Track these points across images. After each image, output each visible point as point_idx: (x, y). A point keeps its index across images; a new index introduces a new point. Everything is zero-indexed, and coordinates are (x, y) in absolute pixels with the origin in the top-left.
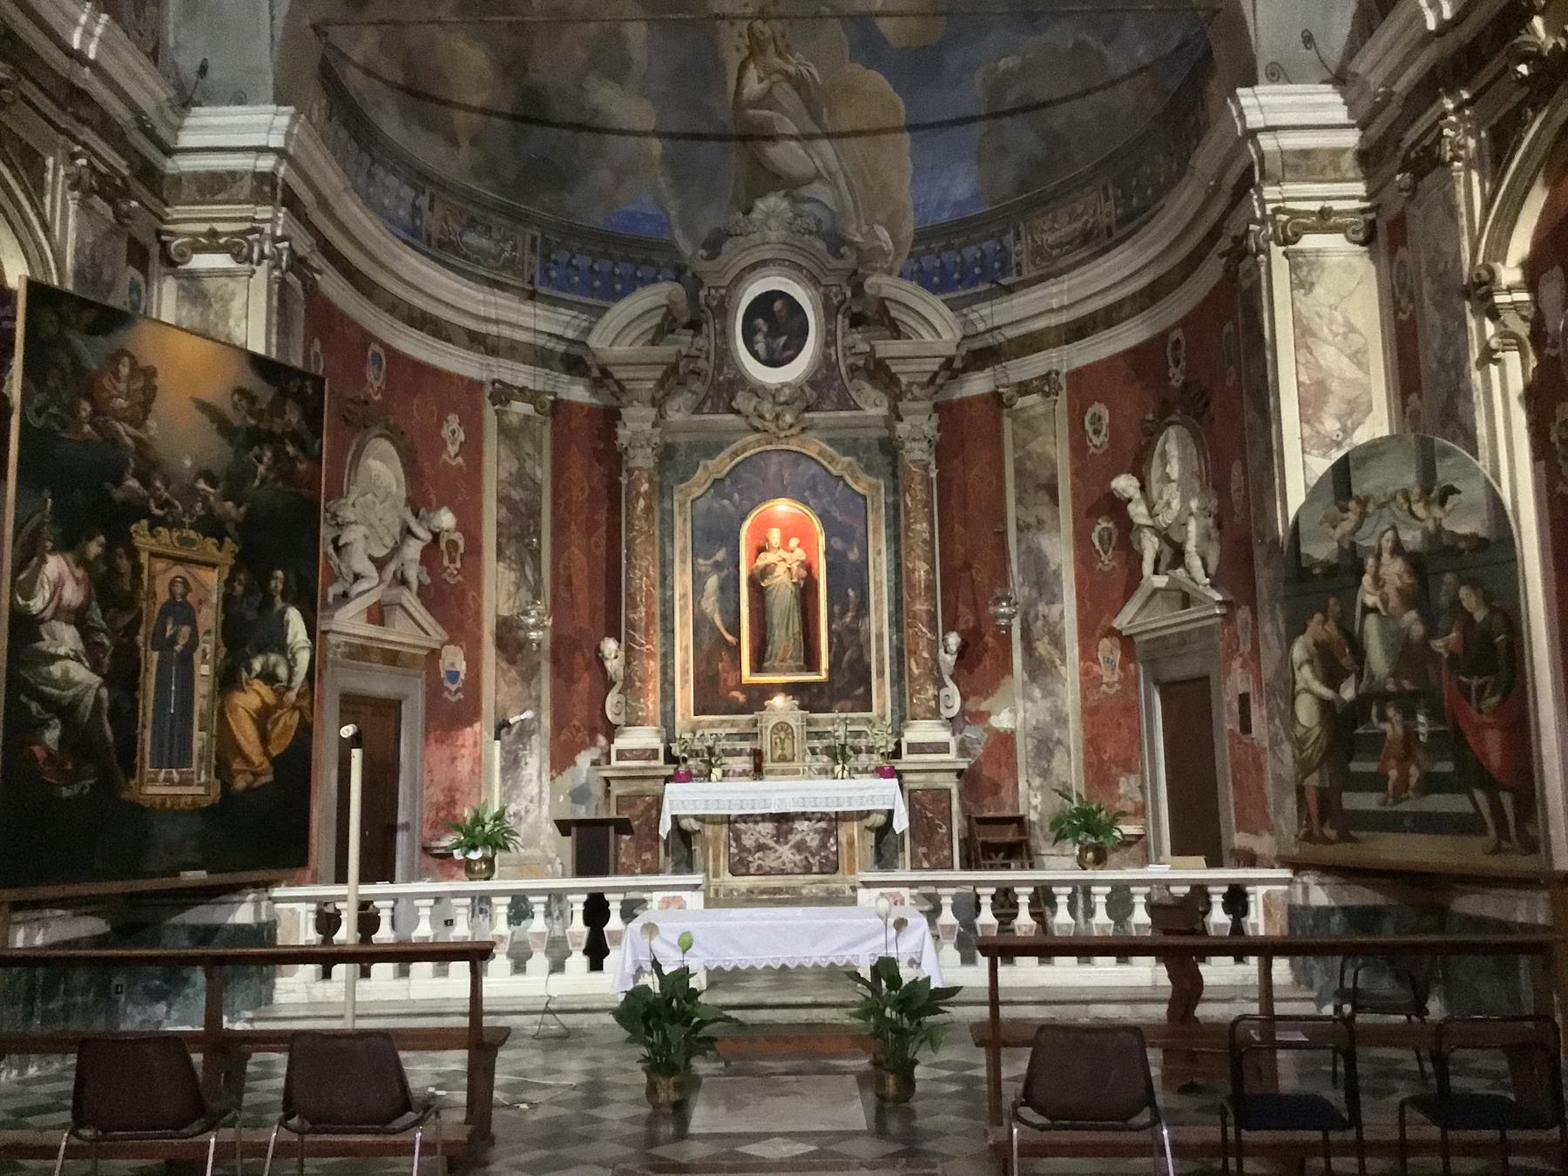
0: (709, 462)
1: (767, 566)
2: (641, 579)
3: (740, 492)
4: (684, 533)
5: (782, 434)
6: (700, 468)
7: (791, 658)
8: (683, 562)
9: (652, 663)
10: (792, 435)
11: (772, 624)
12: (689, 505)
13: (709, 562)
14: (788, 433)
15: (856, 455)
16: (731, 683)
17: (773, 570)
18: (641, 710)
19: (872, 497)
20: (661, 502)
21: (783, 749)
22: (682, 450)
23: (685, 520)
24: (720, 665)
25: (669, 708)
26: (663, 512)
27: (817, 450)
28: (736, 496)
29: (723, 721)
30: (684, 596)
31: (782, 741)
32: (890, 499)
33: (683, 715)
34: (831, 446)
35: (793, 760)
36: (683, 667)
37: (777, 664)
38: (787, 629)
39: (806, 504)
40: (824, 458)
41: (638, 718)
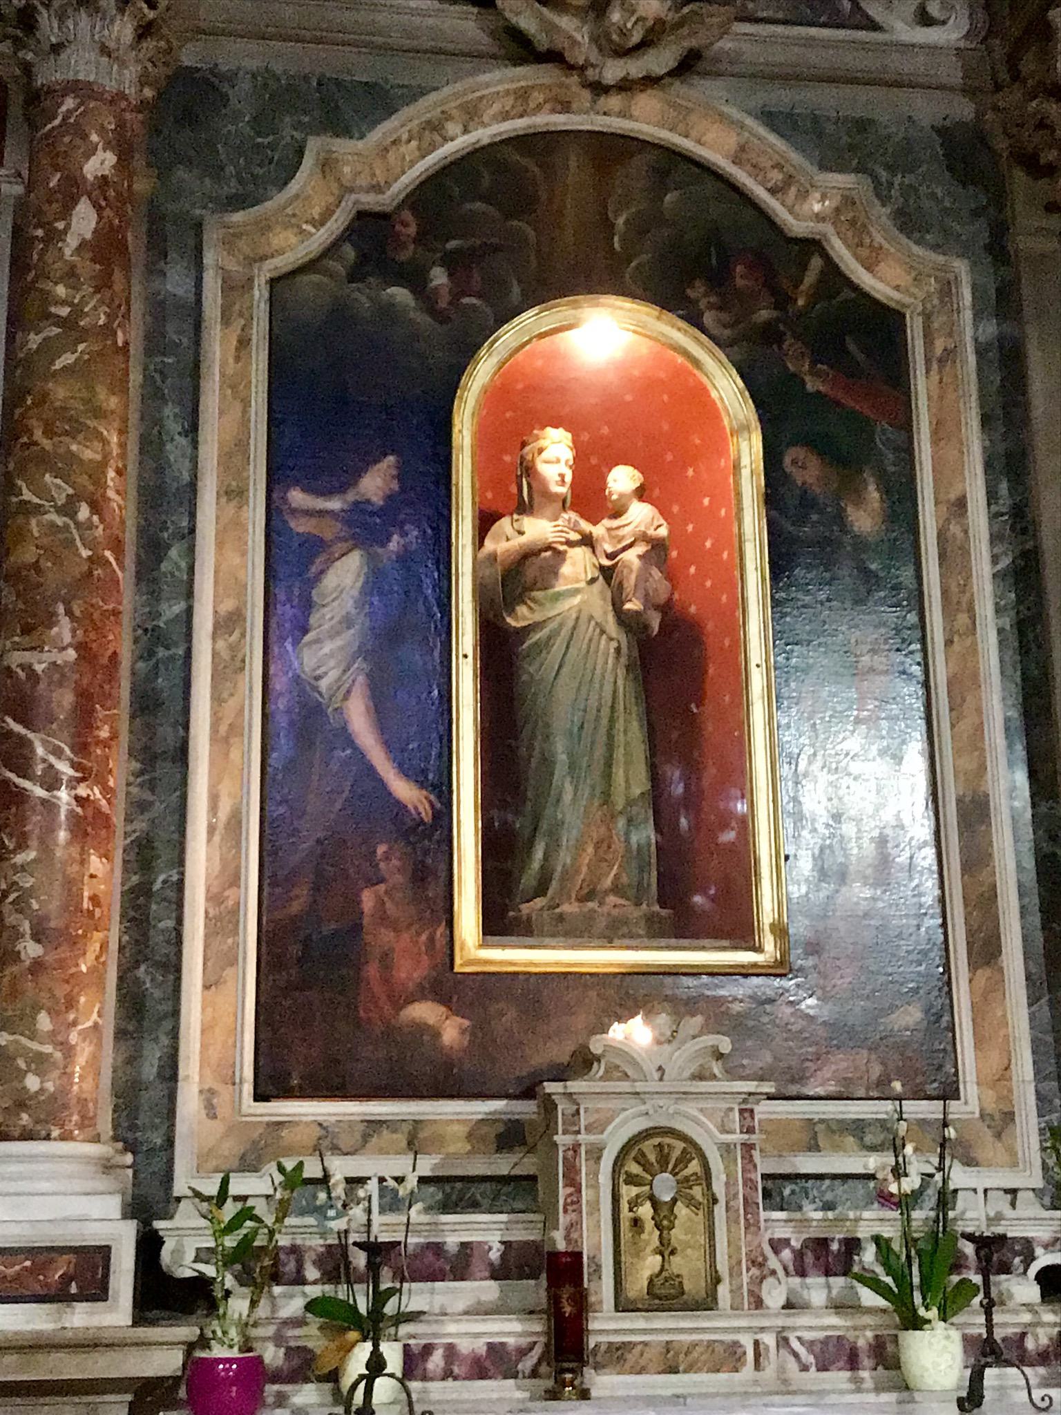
0: (343, 147)
1: (528, 555)
2: (68, 510)
3: (452, 262)
4: (236, 387)
5: (613, 71)
6: (308, 161)
7: (616, 889)
8: (234, 494)
9: (96, 864)
10: (650, 81)
11: (548, 762)
12: (260, 293)
13: (335, 504)
14: (634, 68)
15: (860, 169)
16: (410, 971)
17: (552, 571)
18: (40, 1063)
19: (927, 317)
20: (154, 271)
21: (666, 1249)
22: (241, 96)
23: (244, 343)
24: (368, 900)
25: (150, 1070)
26: (159, 309)
27: (731, 141)
28: (439, 277)
29: (374, 1126)
30: (228, 623)
31: (664, 1215)
32: (990, 329)
33: (209, 1096)
34: (774, 129)
35: (707, 1303)
36: (214, 898)
37: (569, 908)
38: (608, 776)
39: (695, 320)
40: (756, 170)
41: (22, 1103)
